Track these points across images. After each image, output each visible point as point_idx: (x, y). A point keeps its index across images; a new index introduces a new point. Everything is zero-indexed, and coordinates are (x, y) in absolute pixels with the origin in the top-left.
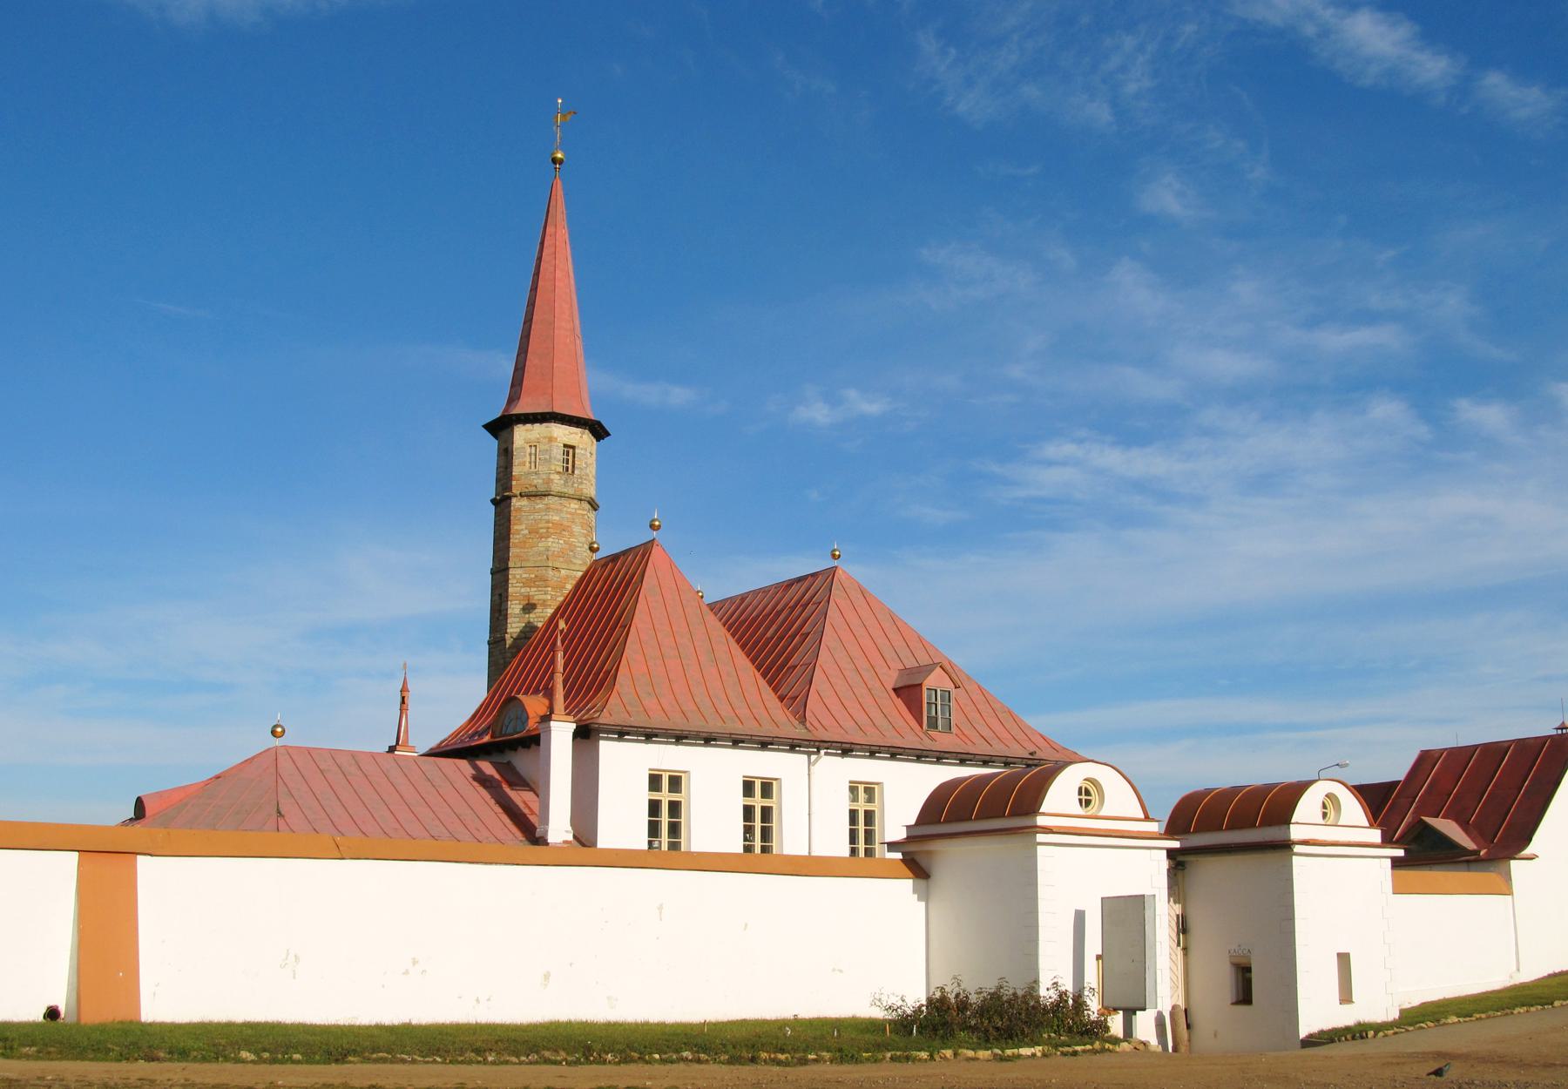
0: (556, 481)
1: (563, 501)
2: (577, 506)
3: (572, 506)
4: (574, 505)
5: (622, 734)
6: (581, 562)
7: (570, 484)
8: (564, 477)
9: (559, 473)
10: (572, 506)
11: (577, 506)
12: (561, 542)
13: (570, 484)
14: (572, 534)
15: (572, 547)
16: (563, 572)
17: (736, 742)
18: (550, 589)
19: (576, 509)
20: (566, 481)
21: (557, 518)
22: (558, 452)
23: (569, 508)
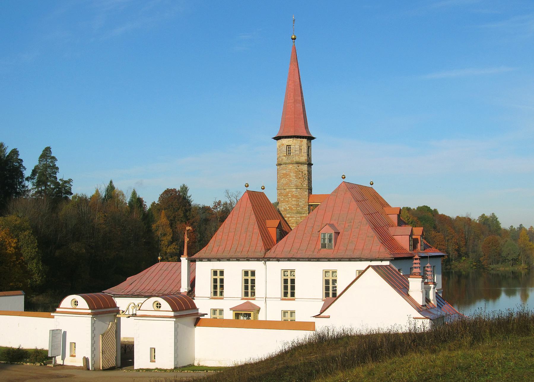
0: (284, 159)
1: (287, 165)
2: (292, 166)
3: (290, 166)
4: (291, 166)
5: (201, 260)
6: (294, 185)
7: (289, 159)
8: (287, 157)
9: (285, 156)
10: (290, 166)
11: (292, 166)
12: (287, 180)
13: (289, 159)
14: (290, 177)
15: (290, 181)
16: (287, 190)
17: (238, 260)
18: (283, 197)
19: (291, 167)
20: (288, 158)
21: (284, 172)
22: (284, 149)
23: (289, 167)
